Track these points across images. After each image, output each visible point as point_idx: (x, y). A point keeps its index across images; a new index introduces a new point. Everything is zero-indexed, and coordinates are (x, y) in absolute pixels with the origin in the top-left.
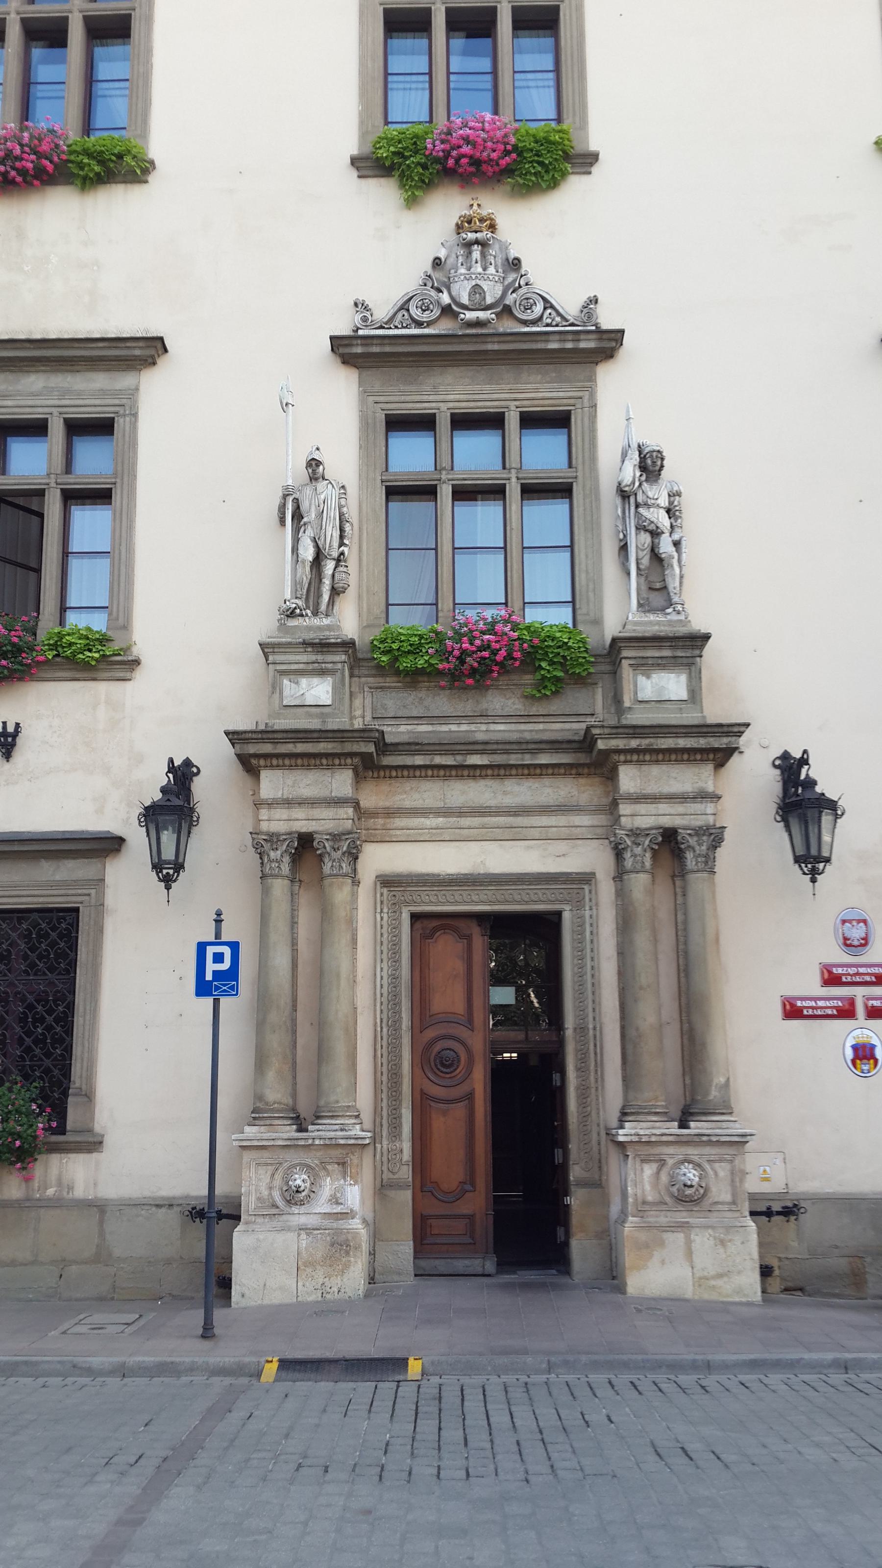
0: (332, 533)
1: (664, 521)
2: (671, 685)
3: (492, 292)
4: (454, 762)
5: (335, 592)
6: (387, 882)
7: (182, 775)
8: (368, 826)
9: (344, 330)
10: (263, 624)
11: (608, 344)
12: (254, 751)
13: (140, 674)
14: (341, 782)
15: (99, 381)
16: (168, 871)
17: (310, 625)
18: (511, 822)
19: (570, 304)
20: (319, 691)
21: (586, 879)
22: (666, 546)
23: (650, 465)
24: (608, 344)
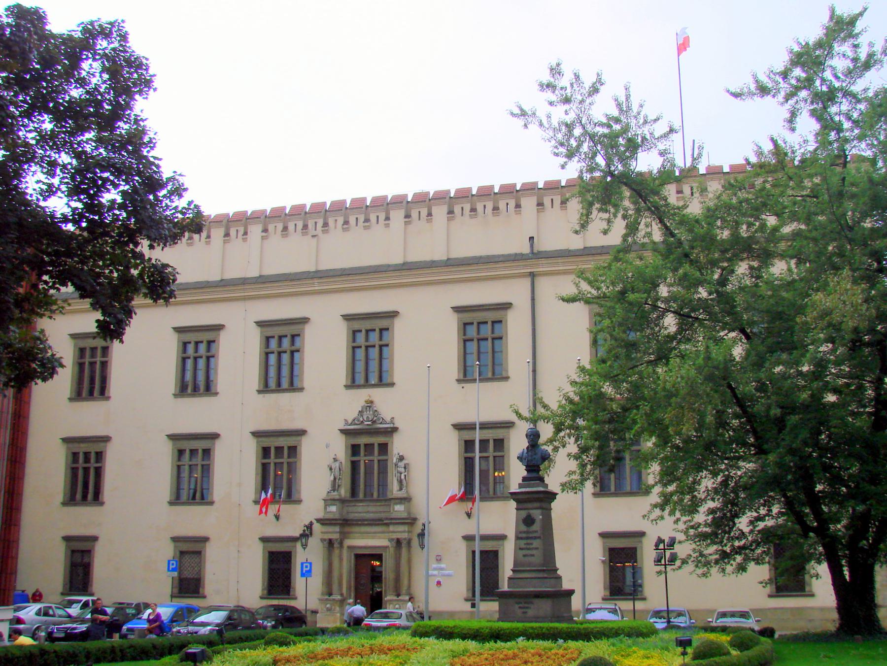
0: (337, 473)
1: (403, 470)
2: (399, 508)
3: (371, 418)
4: (362, 522)
5: (339, 486)
6: (349, 547)
7: (310, 527)
8: (344, 535)
9: (343, 427)
10: (324, 495)
11: (395, 430)
12: (322, 521)
13: (302, 504)
14: (337, 529)
15: (294, 438)
16: (305, 546)
17: (335, 495)
18: (374, 535)
19: (388, 419)
20: (333, 509)
21: (387, 547)
22: (403, 477)
23: (401, 458)
24: (395, 430)
